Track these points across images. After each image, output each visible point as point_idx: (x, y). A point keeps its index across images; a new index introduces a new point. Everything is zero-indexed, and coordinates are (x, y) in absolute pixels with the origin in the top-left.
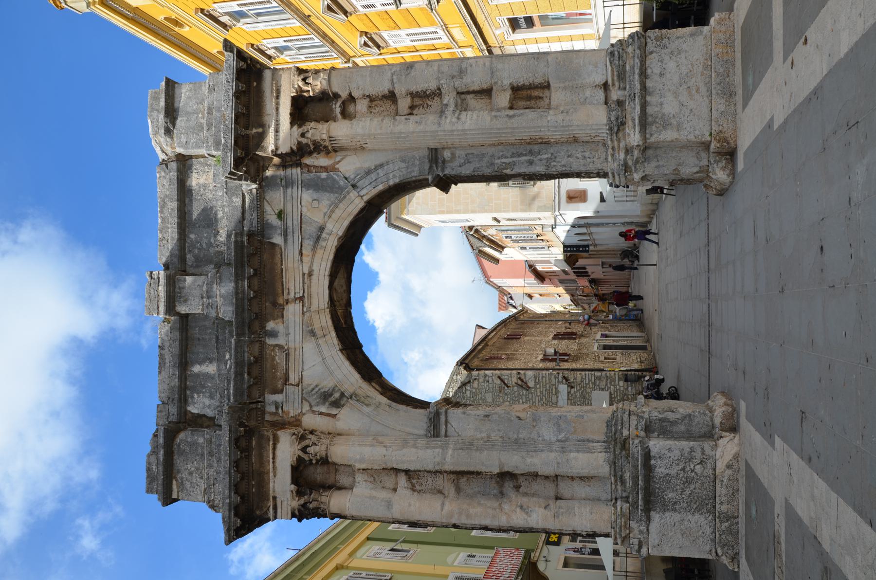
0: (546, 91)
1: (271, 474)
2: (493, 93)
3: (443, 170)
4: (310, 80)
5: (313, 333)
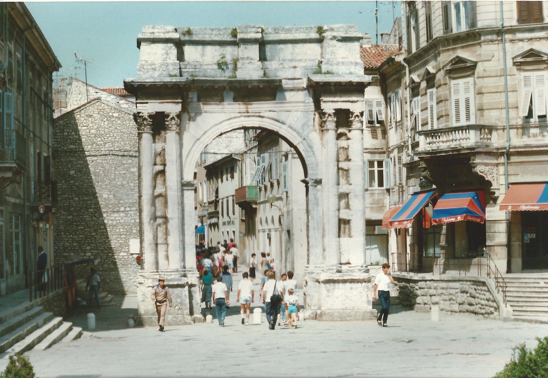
0: (347, 235)
1: (160, 101)
2: (348, 210)
3: (312, 185)
4: (357, 119)
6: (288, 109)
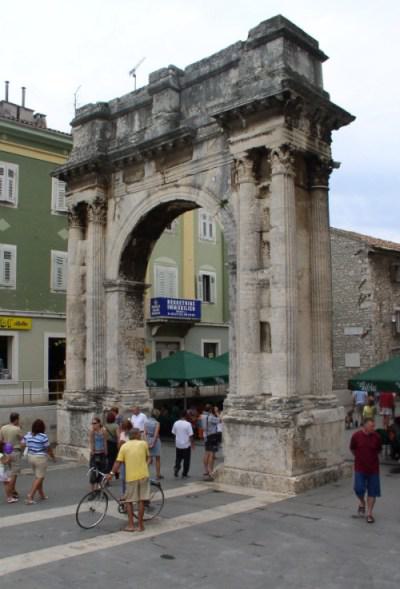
4: (276, 156)
5: (149, 196)
6: (204, 168)
